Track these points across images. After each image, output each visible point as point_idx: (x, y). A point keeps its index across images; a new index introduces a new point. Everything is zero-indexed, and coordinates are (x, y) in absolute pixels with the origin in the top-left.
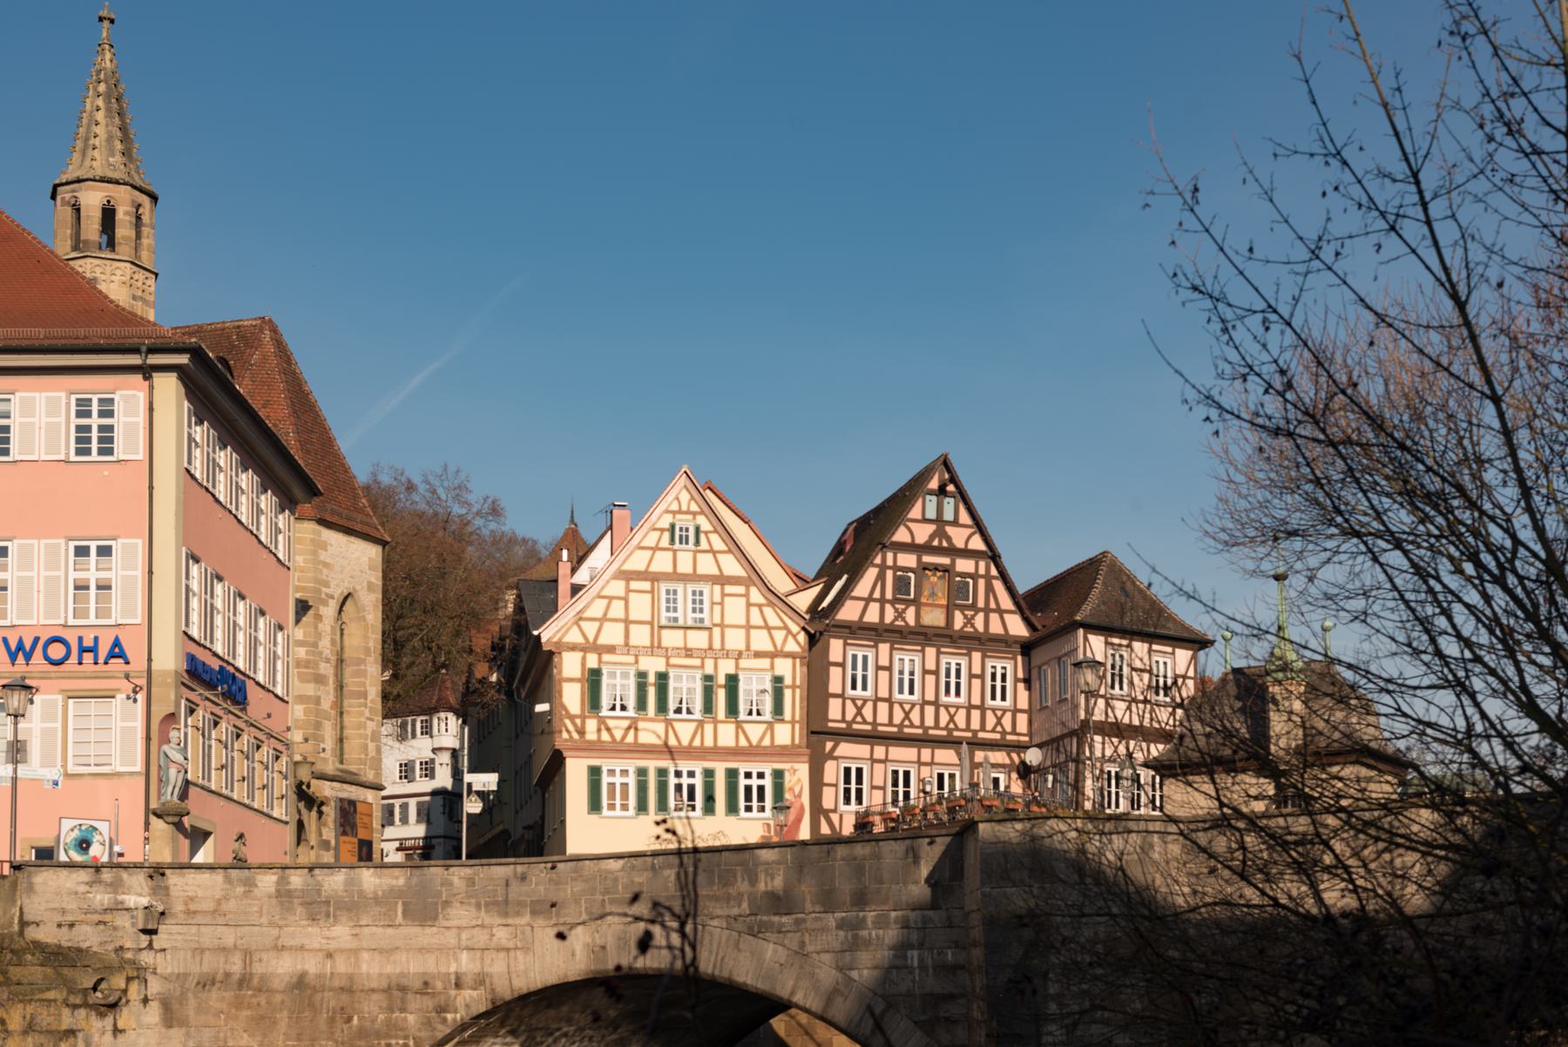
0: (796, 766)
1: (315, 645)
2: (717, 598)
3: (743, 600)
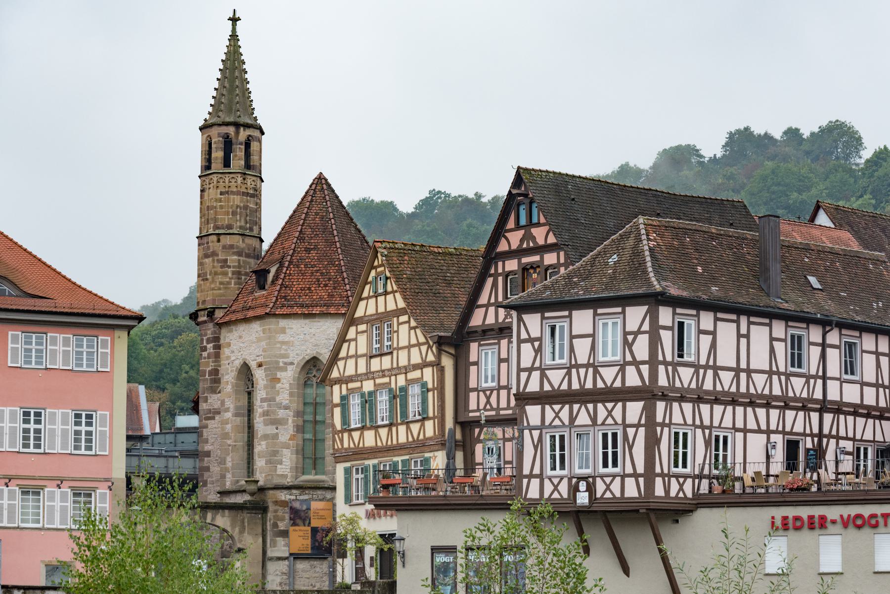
0: (436, 453)
1: (274, 399)
2: (395, 329)
3: (407, 325)
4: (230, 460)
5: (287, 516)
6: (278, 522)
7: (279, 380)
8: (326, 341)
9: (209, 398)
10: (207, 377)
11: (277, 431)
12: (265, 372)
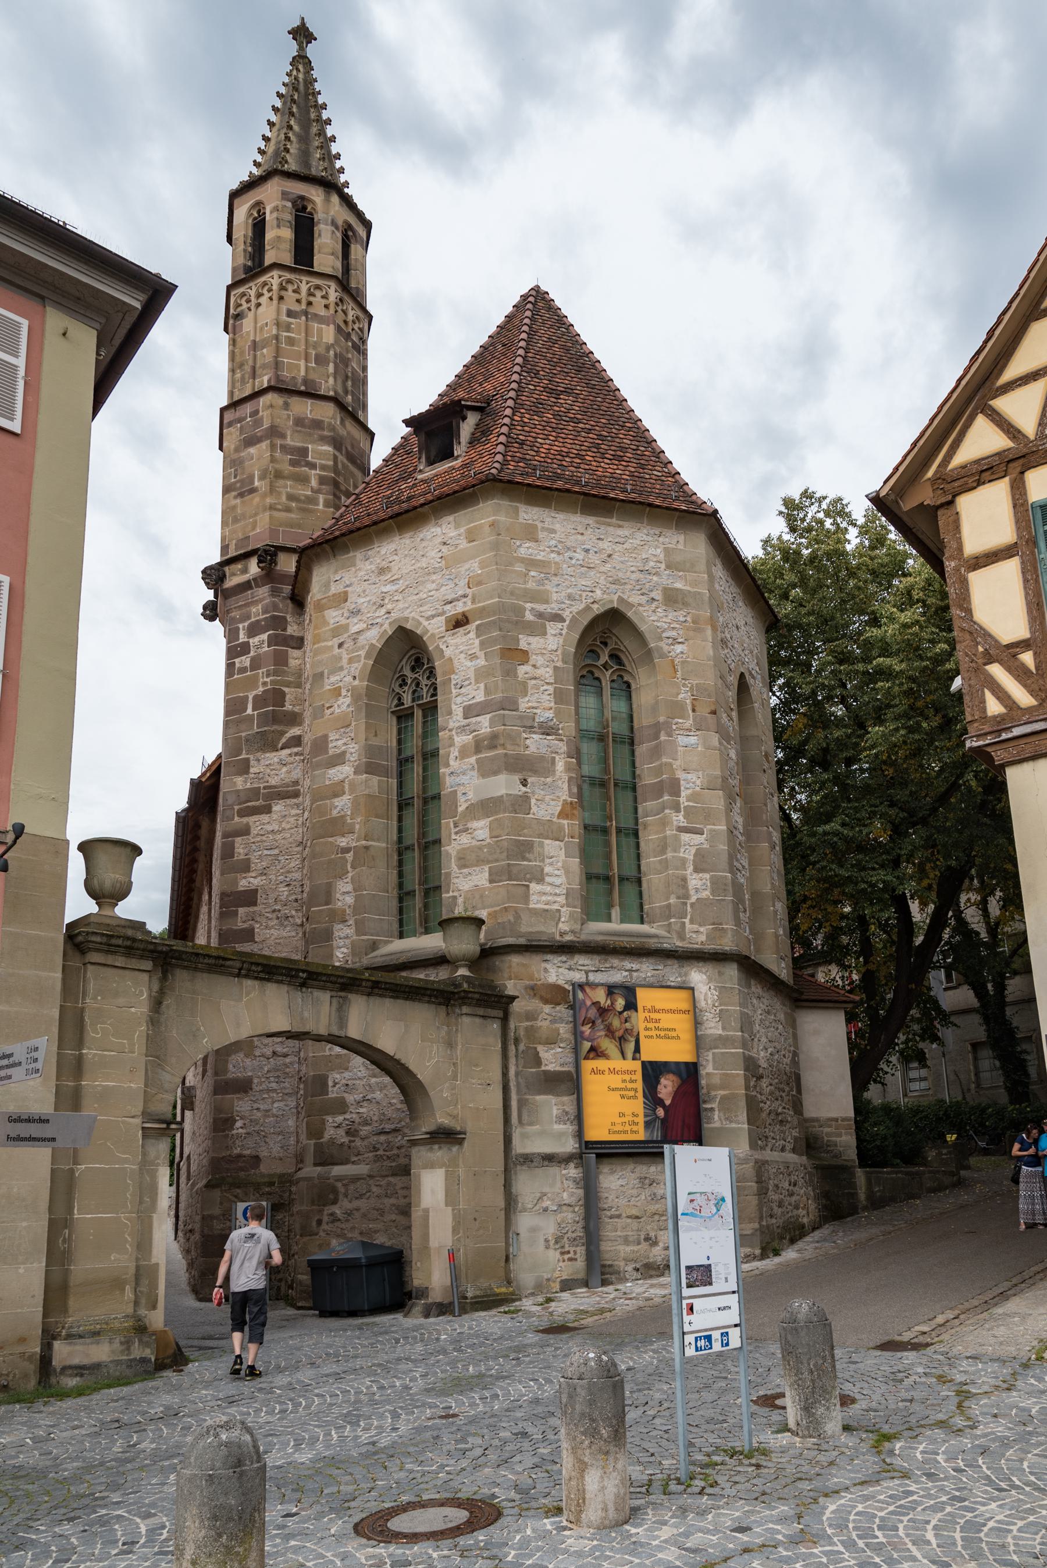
1: (509, 704)
4: (349, 888)
5: (564, 1030)
6: (540, 1049)
7: (524, 656)
8: (638, 575)
9: (252, 763)
10: (249, 711)
11: (524, 789)
12: (478, 636)
